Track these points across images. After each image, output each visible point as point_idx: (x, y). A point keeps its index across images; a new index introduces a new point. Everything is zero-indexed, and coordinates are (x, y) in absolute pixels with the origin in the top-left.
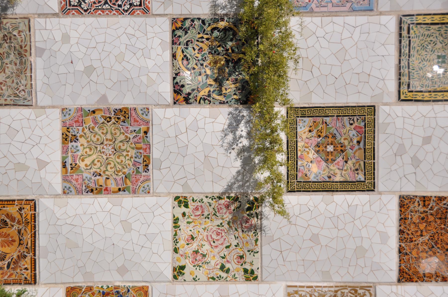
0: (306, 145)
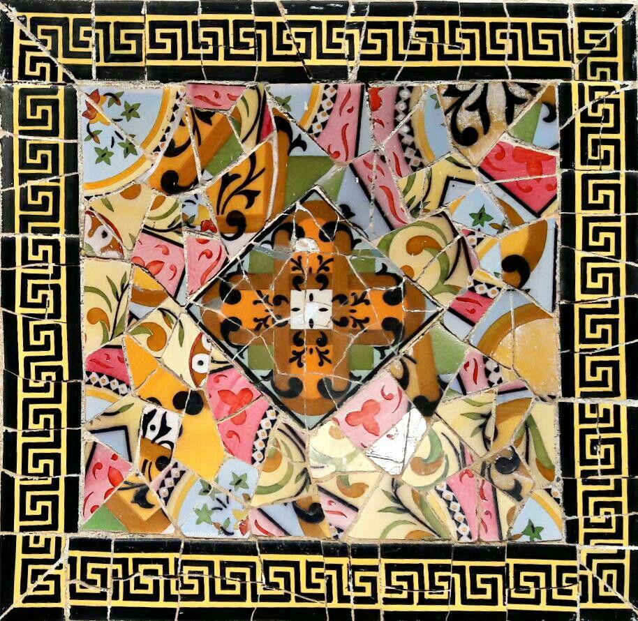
0: (142, 280)
